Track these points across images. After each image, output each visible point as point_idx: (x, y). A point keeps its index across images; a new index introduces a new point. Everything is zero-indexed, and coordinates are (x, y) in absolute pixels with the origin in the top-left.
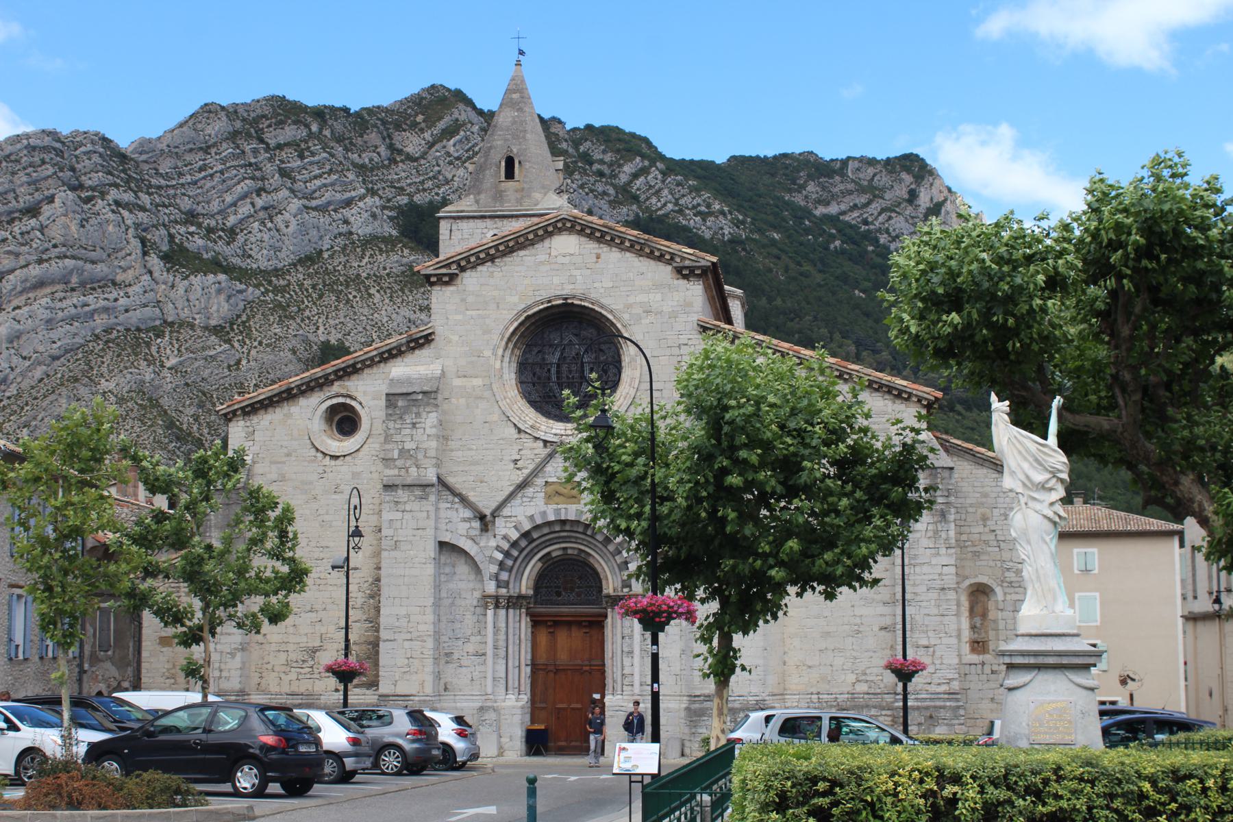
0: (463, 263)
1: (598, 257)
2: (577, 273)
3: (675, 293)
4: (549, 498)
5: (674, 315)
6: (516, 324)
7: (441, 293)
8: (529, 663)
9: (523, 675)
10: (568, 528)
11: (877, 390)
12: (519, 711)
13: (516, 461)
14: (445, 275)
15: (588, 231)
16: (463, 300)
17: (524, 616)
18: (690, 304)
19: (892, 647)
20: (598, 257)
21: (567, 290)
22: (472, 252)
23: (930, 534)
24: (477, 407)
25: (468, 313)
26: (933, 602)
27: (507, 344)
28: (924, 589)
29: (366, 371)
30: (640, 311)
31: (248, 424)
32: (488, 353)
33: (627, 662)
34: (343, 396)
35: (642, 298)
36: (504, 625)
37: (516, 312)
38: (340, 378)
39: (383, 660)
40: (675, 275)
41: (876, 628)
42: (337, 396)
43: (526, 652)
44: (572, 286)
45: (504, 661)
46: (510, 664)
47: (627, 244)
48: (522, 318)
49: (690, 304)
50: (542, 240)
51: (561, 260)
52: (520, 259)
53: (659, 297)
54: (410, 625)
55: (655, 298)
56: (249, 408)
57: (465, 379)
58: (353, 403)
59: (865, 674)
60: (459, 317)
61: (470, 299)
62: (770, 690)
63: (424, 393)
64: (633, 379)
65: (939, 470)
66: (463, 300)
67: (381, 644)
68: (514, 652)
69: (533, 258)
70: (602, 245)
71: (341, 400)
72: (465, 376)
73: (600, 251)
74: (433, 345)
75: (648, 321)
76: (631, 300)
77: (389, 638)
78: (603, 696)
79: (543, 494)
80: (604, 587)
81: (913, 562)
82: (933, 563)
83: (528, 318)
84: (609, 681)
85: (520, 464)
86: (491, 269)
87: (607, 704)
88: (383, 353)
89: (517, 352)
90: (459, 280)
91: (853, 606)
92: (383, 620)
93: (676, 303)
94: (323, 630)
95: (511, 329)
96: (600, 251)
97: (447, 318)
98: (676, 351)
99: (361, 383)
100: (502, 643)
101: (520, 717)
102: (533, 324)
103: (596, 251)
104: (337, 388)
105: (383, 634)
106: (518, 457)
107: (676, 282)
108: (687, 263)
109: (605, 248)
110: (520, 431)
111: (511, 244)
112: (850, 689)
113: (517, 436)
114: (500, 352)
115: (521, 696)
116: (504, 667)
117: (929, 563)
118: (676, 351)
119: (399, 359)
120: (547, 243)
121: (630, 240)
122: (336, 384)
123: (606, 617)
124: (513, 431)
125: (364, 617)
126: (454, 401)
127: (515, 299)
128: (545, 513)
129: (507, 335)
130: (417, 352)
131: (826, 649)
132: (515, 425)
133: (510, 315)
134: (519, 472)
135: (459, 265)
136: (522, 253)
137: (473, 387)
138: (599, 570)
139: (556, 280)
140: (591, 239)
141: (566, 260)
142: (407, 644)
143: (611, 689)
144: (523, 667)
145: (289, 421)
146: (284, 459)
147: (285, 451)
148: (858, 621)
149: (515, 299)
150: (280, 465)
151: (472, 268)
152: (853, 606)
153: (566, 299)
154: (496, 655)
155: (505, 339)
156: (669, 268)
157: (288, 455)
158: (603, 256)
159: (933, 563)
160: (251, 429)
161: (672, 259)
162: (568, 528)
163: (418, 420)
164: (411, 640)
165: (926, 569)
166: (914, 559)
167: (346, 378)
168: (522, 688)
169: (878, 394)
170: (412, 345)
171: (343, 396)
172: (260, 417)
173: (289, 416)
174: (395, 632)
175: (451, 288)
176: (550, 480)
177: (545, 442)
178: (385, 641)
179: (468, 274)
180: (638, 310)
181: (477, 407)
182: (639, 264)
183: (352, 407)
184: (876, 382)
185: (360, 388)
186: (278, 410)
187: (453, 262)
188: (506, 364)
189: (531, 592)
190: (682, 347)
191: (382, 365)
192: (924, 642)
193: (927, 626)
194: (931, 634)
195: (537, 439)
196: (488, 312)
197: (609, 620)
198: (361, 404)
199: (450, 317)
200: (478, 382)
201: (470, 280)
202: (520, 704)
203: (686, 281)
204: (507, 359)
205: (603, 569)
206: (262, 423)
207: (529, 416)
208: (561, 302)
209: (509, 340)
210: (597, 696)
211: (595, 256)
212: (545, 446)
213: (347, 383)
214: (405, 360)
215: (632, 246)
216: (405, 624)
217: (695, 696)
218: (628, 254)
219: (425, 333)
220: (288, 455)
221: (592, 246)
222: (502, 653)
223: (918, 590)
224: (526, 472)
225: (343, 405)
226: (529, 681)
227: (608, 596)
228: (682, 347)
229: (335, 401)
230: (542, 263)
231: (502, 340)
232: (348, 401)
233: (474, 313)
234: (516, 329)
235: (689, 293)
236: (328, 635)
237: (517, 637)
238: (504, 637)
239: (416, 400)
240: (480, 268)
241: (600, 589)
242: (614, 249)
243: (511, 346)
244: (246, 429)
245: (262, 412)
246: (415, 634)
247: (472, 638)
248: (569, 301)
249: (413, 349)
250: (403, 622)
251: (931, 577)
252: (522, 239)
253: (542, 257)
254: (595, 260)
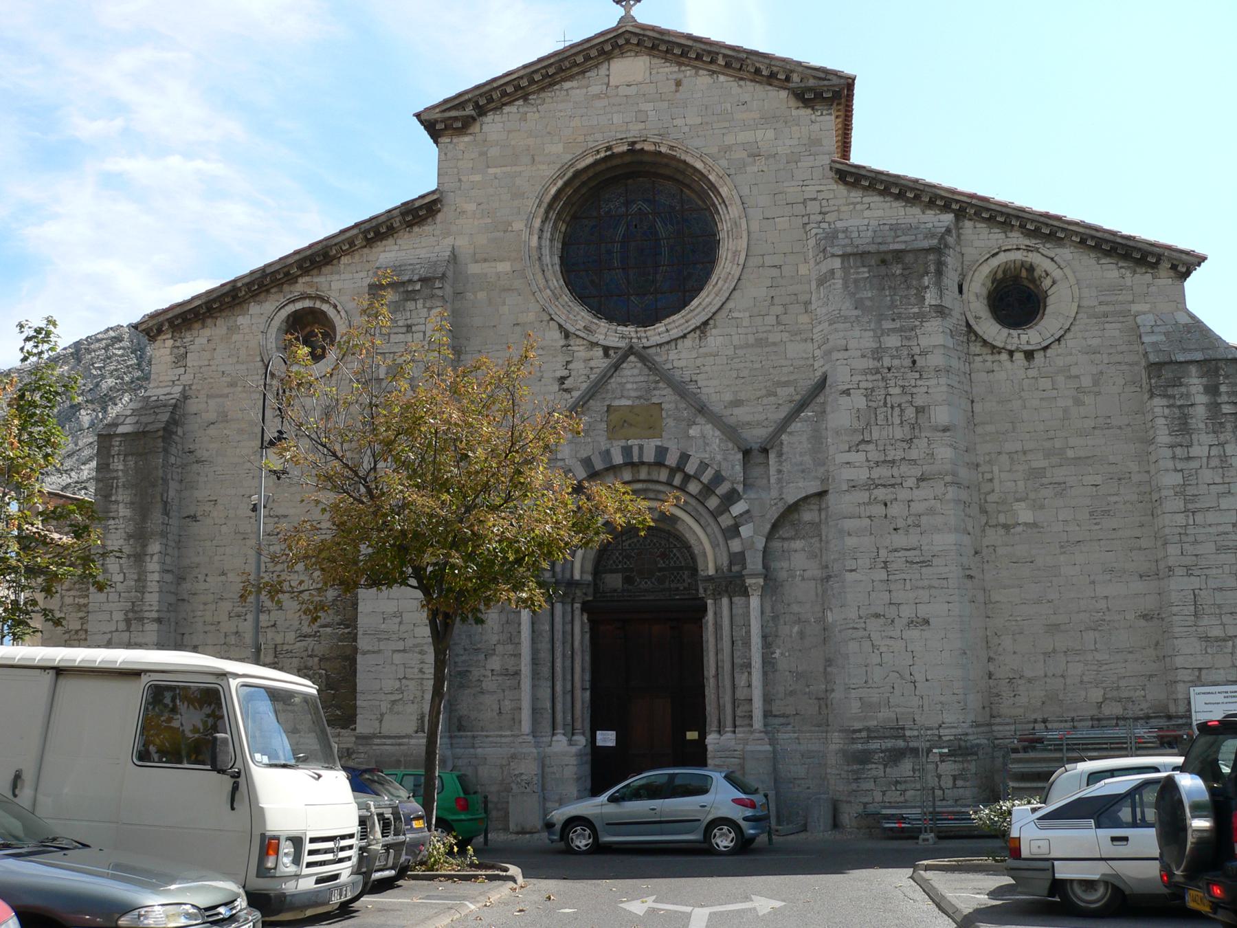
0: (482, 102)
1: (678, 83)
2: (650, 106)
3: (794, 128)
4: (613, 431)
5: (794, 159)
6: (560, 183)
7: (450, 146)
8: (588, 685)
9: (578, 706)
10: (643, 474)
11: (1107, 254)
12: (573, 761)
13: (562, 380)
14: (456, 119)
15: (663, 48)
16: (483, 154)
17: (577, 612)
18: (818, 142)
19: (1157, 644)
20: (678, 83)
21: (634, 131)
22: (495, 85)
23: (1215, 462)
24: (504, 304)
25: (491, 171)
26: (1227, 568)
27: (547, 212)
28: (1211, 547)
29: (344, 260)
30: (744, 155)
31: (178, 344)
32: (519, 225)
33: (741, 680)
34: (310, 297)
35: (745, 136)
36: (547, 627)
37: (559, 166)
38: (306, 272)
39: (362, 681)
40: (793, 103)
41: (1130, 616)
42: (303, 297)
43: (583, 670)
44: (642, 126)
45: (549, 684)
46: (559, 688)
47: (721, 61)
48: (569, 174)
49: (818, 142)
50: (596, 66)
51: (623, 91)
52: (564, 93)
53: (770, 134)
54: (403, 628)
55: (765, 136)
56: (180, 321)
57: (486, 265)
58: (325, 307)
59: (1118, 688)
60: (478, 178)
61: (494, 152)
62: (971, 717)
63: (423, 280)
64: (736, 253)
65: (1221, 364)
66: (483, 154)
67: (359, 658)
68: (564, 668)
69: (584, 90)
70: (683, 68)
71: (307, 304)
72: (485, 260)
73: (681, 76)
74: (439, 216)
75: (756, 169)
76: (730, 140)
77: (370, 648)
78: (703, 736)
79: (604, 426)
80: (700, 567)
81: (1190, 506)
82: (1223, 506)
83: (577, 174)
84: (711, 708)
85: (568, 383)
86: (521, 110)
87: (710, 748)
88: (368, 231)
89: (563, 227)
90: (476, 128)
91: (1093, 582)
92: (362, 621)
93: (795, 142)
94: (279, 640)
95: (553, 191)
96: (681, 76)
97: (460, 180)
98: (799, 209)
99: (336, 277)
100: (545, 655)
101: (575, 769)
102: (584, 183)
103: (675, 76)
104: (301, 286)
105: (362, 643)
106: (565, 373)
107: (794, 112)
108: (811, 82)
109: (689, 72)
110: (567, 335)
111: (551, 71)
112: (1094, 712)
113: (563, 342)
114: (537, 223)
115: (575, 738)
116: (549, 691)
117: (1217, 509)
118: (799, 209)
119: (390, 241)
120: (603, 70)
121: (725, 56)
122: (301, 280)
123: (704, 609)
124: (557, 335)
125: (338, 619)
126: (469, 295)
127: (559, 148)
128: (608, 452)
129: (548, 199)
130: (416, 229)
131: (1054, 651)
132: (560, 326)
133: (548, 171)
134: (567, 396)
135: (477, 106)
136: (567, 85)
137: (498, 275)
138: (692, 541)
139: (617, 119)
140: (667, 60)
141: (632, 91)
142: (398, 658)
143: (715, 723)
144: (578, 693)
145: (235, 337)
146: (226, 391)
147: (229, 379)
148: (1102, 604)
149: (559, 148)
150: (218, 400)
151: (495, 109)
152: (1093, 582)
153: (634, 143)
154: (535, 675)
155: (545, 205)
156: (783, 94)
157: (232, 384)
158: (685, 82)
159: (1223, 506)
160: (182, 350)
161: (788, 79)
162: (643, 474)
163: (415, 321)
164: (404, 651)
165: (1211, 517)
166: (1193, 502)
167: (315, 272)
168: (578, 725)
169: (1108, 260)
170: (410, 218)
171: (310, 297)
172: (195, 333)
173: (233, 329)
174: (379, 640)
175: (466, 139)
176: (616, 403)
177: (606, 350)
178: (365, 653)
179: (489, 118)
180: (740, 154)
181: (504, 304)
182: (740, 90)
183: (324, 313)
184: (1107, 241)
185: (335, 286)
186: (219, 322)
187: (469, 100)
188: (546, 243)
189: (589, 578)
190: (809, 203)
191: (366, 250)
192: (1217, 632)
193: (1219, 606)
194: (1226, 619)
195: (594, 344)
196: (515, 169)
197: (710, 616)
198: (335, 307)
199: (464, 179)
200: (503, 267)
201: (493, 126)
202: (574, 749)
203: (809, 111)
204: (547, 235)
205: (698, 539)
206: (198, 341)
207: (579, 317)
208: (625, 148)
209: (550, 206)
210: (692, 735)
211: (673, 82)
212: (606, 355)
213: (316, 280)
214: (399, 242)
215: (728, 65)
216: (396, 627)
217: (855, 731)
218: (722, 78)
219: (427, 200)
220: (232, 384)
221: (667, 70)
222: (546, 671)
223: (1200, 549)
224: (576, 394)
225: (312, 311)
226: (587, 716)
227: (710, 579)
228: (809, 203)
229: (299, 306)
230: (598, 97)
231: (539, 206)
232: (318, 305)
233: (498, 170)
234: (559, 192)
235: (816, 127)
236: (285, 647)
237: (568, 646)
238: (549, 646)
239: (414, 291)
240: (506, 109)
241: (694, 570)
242: (701, 72)
243: (553, 215)
244: (176, 351)
245: (197, 326)
246: (410, 642)
247: (500, 648)
248: (638, 147)
249: (410, 225)
250: (392, 625)
251: (1221, 529)
252: (567, 64)
253: (595, 89)
254: (674, 88)
